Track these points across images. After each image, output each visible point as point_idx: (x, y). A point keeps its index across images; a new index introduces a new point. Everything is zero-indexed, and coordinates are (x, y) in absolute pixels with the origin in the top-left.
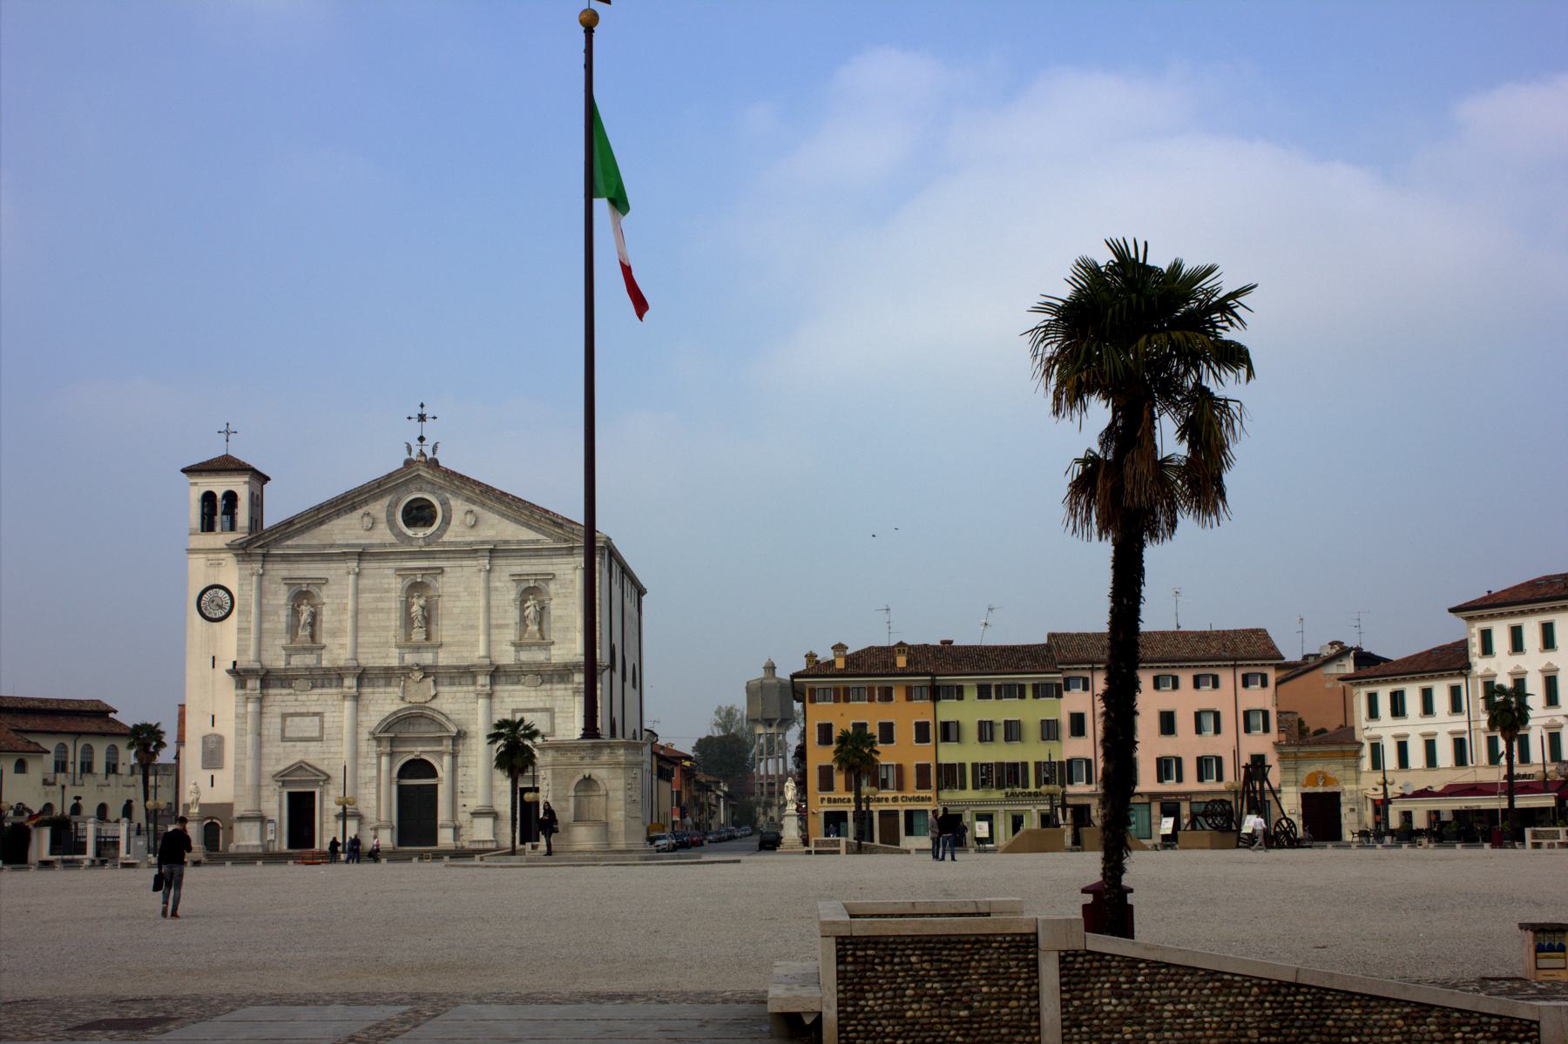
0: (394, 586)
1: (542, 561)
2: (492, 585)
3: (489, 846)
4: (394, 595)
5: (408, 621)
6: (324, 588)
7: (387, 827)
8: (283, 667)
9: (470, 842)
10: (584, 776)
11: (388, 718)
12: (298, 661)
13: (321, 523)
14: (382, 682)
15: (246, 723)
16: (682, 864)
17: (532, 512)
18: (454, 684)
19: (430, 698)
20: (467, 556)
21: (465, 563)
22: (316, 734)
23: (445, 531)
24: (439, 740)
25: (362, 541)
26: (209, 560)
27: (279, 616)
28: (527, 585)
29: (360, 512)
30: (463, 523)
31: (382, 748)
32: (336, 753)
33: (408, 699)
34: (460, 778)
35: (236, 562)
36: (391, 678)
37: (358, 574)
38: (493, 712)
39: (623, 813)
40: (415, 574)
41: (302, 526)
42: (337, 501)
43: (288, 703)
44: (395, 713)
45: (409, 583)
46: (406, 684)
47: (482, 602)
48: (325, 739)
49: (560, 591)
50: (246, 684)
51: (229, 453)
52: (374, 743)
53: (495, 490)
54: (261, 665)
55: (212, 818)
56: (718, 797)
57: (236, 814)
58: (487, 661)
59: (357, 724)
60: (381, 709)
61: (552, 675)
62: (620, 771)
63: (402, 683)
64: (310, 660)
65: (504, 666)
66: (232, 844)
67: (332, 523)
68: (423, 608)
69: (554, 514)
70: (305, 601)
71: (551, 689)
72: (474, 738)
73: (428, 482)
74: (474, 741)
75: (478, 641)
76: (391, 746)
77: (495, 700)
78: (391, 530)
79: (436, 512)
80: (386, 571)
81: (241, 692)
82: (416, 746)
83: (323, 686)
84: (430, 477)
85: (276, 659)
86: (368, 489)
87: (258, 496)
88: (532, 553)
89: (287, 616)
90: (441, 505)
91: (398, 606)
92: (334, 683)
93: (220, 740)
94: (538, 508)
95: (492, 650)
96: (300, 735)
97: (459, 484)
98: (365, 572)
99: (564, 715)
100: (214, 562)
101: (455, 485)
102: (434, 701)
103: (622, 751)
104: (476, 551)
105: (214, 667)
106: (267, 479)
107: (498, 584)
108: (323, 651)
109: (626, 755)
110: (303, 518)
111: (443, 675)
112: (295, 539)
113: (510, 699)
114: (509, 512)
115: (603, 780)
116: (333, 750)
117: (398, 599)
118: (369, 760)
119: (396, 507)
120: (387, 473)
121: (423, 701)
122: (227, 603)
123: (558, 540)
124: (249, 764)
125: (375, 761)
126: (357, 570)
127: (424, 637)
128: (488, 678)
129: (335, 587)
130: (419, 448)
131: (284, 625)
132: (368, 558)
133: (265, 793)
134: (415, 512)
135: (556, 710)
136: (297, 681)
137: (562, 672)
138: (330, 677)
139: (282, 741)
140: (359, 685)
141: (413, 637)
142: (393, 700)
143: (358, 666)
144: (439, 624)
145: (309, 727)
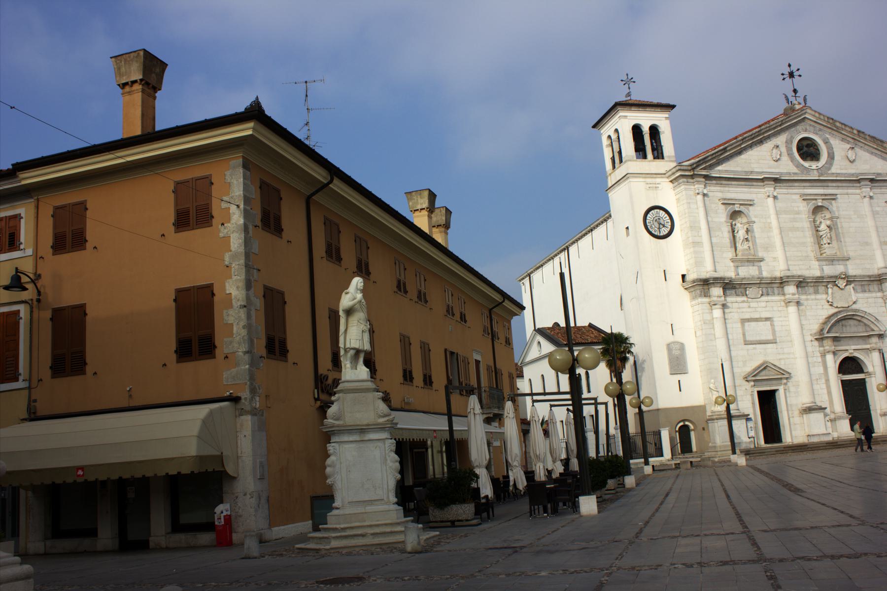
0: (801, 208)
14: (811, 290)
18: (865, 291)
20: (851, 185)
21: (850, 191)
22: (770, 337)
23: (831, 164)
26: (648, 184)
27: (722, 233)
32: (789, 354)
40: (816, 199)
43: (744, 310)
45: (813, 207)
48: (778, 341)
55: (684, 421)
67: (748, 153)
78: (792, 161)
82: (849, 345)
83: (768, 295)
85: (728, 271)
89: (729, 232)
91: (809, 226)
93: (682, 347)
96: (758, 338)
112: (724, 165)
118: (815, 359)
121: (847, 306)
122: (668, 222)
125: (820, 359)
136: (751, 289)
142: (823, 306)
144: (842, 240)
145: (761, 331)
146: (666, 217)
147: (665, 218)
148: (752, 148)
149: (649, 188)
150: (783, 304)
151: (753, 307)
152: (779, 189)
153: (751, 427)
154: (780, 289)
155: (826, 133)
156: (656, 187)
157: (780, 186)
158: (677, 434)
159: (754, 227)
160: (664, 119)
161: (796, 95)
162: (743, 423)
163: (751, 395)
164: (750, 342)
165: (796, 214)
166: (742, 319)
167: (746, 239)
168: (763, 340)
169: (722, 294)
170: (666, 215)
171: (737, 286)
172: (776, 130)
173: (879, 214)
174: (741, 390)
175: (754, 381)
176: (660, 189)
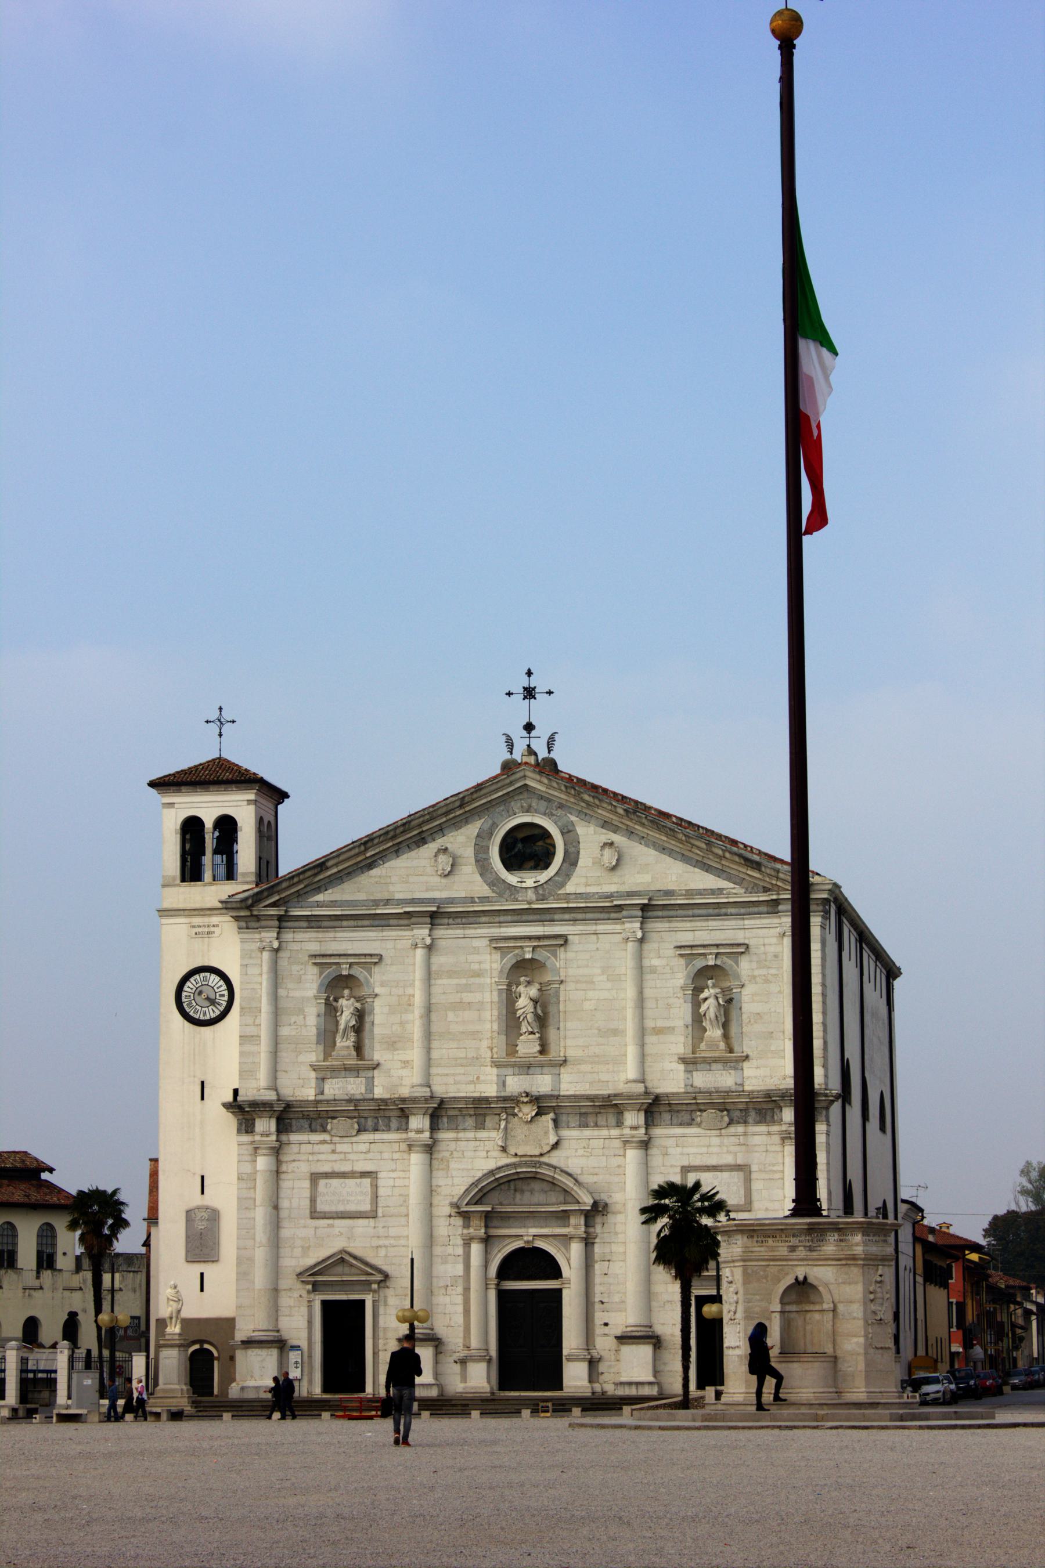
0: (487, 966)
1: (727, 923)
2: (646, 963)
3: (646, 1391)
4: (488, 981)
5: (511, 1022)
6: (376, 969)
7: (480, 1359)
8: (312, 1098)
9: (616, 1384)
10: (796, 1279)
11: (479, 1180)
12: (335, 1088)
13: (370, 866)
14: (470, 1122)
15: (254, 1188)
16: (963, 1427)
17: (709, 844)
19: (548, 1148)
20: (606, 916)
21: (601, 927)
22: (366, 1207)
23: (568, 876)
24: (563, 1217)
25: (436, 895)
26: (194, 927)
27: (304, 1018)
28: (704, 964)
29: (432, 847)
30: (597, 862)
31: (471, 1230)
32: (395, 1238)
33: (512, 1150)
34: (598, 1279)
35: (236, 928)
36: (485, 1115)
37: (430, 948)
38: (650, 1170)
39: (862, 1340)
40: (521, 947)
41: (339, 871)
42: (396, 828)
43: (322, 1157)
44: (492, 1172)
45: (514, 961)
46: (510, 1126)
47: (630, 993)
48: (380, 1214)
49: (756, 973)
50: (253, 1124)
51: (224, 755)
52: (459, 1221)
53: (650, 808)
54: (278, 1094)
55: (201, 1342)
56: (1028, 1313)
57: (240, 1336)
58: (640, 1088)
59: (432, 1191)
60: (470, 1167)
61: (746, 1110)
62: (855, 1270)
63: (503, 1124)
64: (354, 1087)
65: (667, 1095)
66: (234, 1384)
67: (386, 865)
68: (535, 1002)
69: (745, 846)
70: (346, 992)
71: (745, 1134)
72: (620, 1213)
73: (542, 798)
74: (620, 1218)
75: (626, 1055)
76: (486, 1227)
77: (653, 1151)
78: (481, 875)
79: (554, 846)
80: (476, 943)
81: (246, 1138)
83: (376, 1130)
84: (544, 789)
86: (444, 810)
87: (269, 823)
88: (711, 911)
89: (319, 1016)
90: (563, 834)
91: (496, 999)
92: (394, 1123)
93: (214, 1216)
94: (719, 837)
95: (647, 1069)
96: (341, 1208)
97: (590, 799)
98: (442, 943)
99: (767, 1176)
100: (200, 930)
101: (583, 801)
102: (555, 1153)
103: (858, 1238)
104: (620, 908)
105: (202, 1098)
106: (282, 796)
107: (656, 962)
108: (376, 1072)
109: (865, 1244)
110: (342, 858)
111: (569, 1110)
112: (330, 891)
113: (679, 1150)
114: (672, 844)
115: (826, 1285)
116: (393, 1232)
117: (494, 985)
118: (450, 1250)
119: (490, 839)
120: (474, 784)
121: (537, 1153)
122: (223, 996)
123: (753, 888)
124: (260, 1255)
125: (460, 1251)
126: (428, 941)
127: (538, 1048)
128: (642, 1115)
130: (527, 741)
131: (314, 1031)
132: (446, 921)
133: (286, 1301)
134: (520, 845)
135: (754, 1168)
136: (335, 1121)
137: (765, 1106)
138: (387, 1114)
139: (312, 1218)
140: (434, 1128)
141: (518, 1048)
142: (487, 1152)
143: (432, 1097)
146: (221, 986)
147: (218, 988)
151: (341, 1153)
152: (447, 929)
153: (296, 1362)
154: (404, 1120)
155: (571, 813)
156: (209, 933)
159: (375, 1004)
160: (245, 803)
161: (531, 735)
162: (271, 1355)
164: (322, 1215)
165: (472, 977)
166: (312, 1174)
170: (222, 983)
172: (452, 816)
173: (655, 973)
174: (290, 1297)
176: (216, 934)
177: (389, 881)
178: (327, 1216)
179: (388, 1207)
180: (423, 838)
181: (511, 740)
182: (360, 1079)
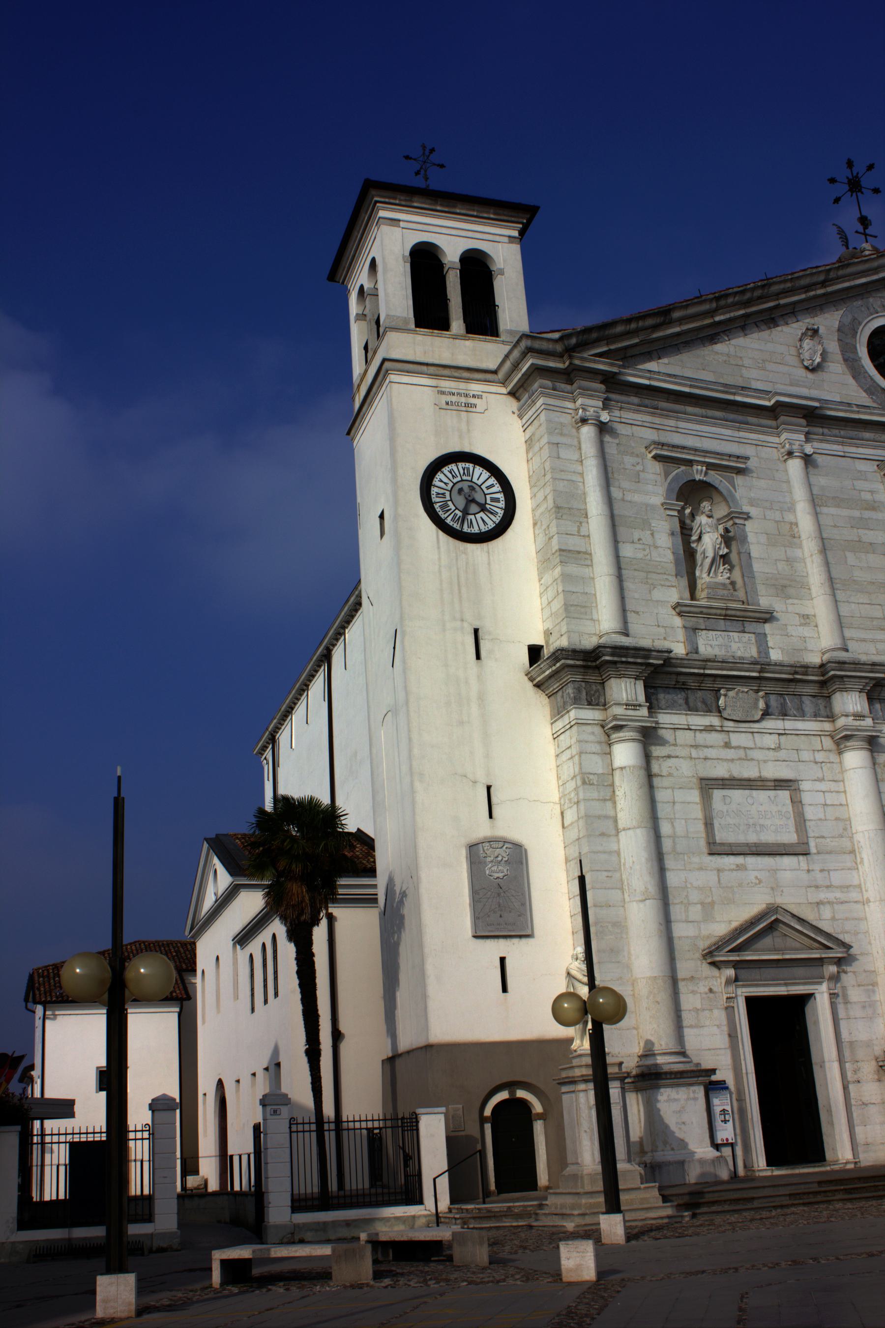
22: (790, 837)
26: (443, 393)
27: (652, 534)
32: (845, 888)
43: (711, 753)
48: (813, 850)
55: (511, 1085)
67: (733, 342)
78: (854, 377)
80: (862, 466)
89: (672, 534)
96: (752, 838)
100: (454, 399)
105: (478, 657)
112: (665, 360)
116: (837, 878)
122: (495, 500)
129: (763, 483)
131: (670, 557)
139: (711, 854)
146: (492, 486)
147: (488, 488)
148: (748, 332)
149: (447, 403)
150: (828, 743)
151: (739, 747)
152: (822, 441)
153: (724, 1112)
154: (821, 702)
156: (467, 405)
157: (823, 434)
158: (488, 1127)
160: (506, 239)
161: (867, 231)
162: (695, 1099)
163: (726, 1008)
164: (726, 849)
165: (866, 509)
167: (722, 556)
168: (767, 845)
169: (642, 698)
171: (692, 683)
172: (812, 293)
174: (693, 992)
175: (736, 965)
176: (478, 409)
177: (740, 363)
178: (735, 851)
179: (823, 837)
180: (773, 319)
181: (843, 232)
182: (747, 635)
